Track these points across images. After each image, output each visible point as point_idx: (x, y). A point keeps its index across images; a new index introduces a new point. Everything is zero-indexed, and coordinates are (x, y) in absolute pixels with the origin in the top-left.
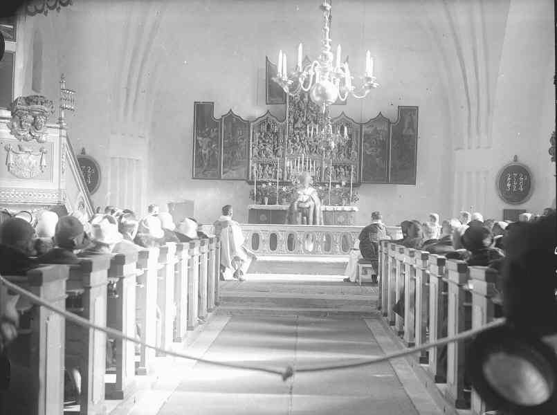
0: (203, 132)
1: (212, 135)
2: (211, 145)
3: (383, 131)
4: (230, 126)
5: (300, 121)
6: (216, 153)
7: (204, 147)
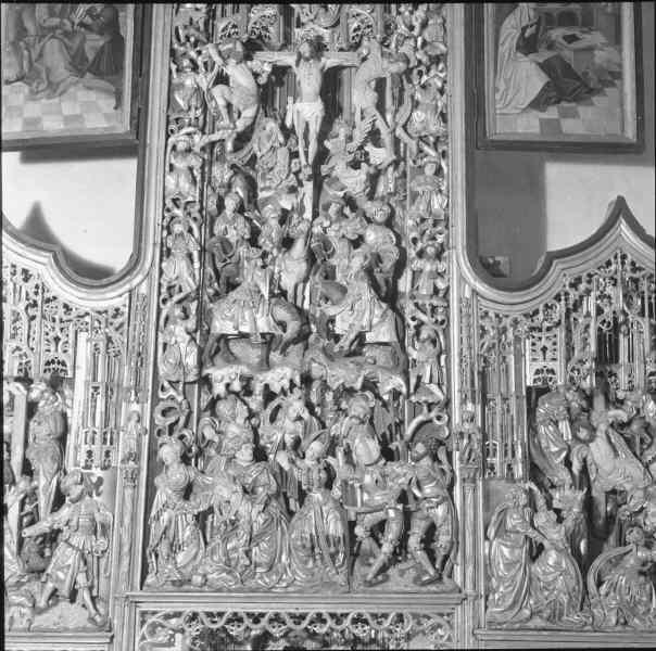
5: (253, 277)
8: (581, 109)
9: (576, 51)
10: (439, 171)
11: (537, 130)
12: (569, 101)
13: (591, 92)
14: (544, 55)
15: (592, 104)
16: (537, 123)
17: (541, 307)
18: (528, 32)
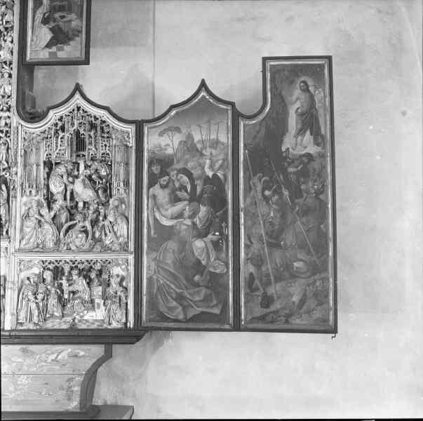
3: (216, 144)
8: (65, 47)
9: (65, 22)
10: (10, 76)
11: (47, 56)
12: (61, 44)
13: (70, 39)
14: (52, 24)
15: (69, 45)
16: (47, 54)
17: (47, 129)
18: (47, 15)
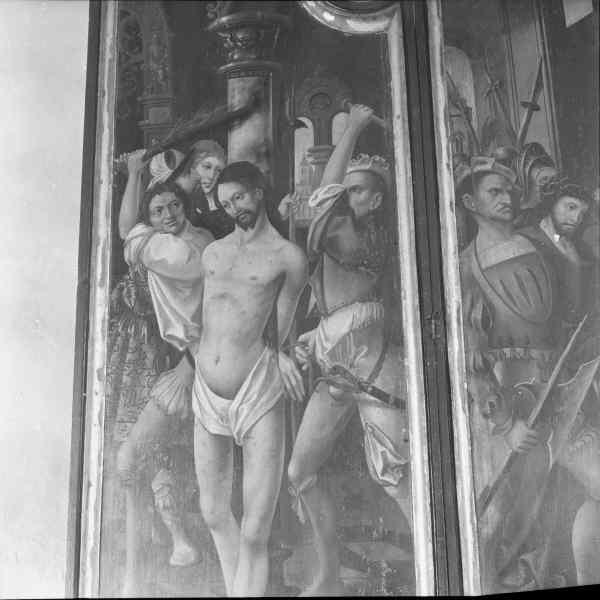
0: (206, 166)
1: (315, 200)
2: (308, 320)
4: (528, 49)
6: (375, 416)
7: (215, 357)
